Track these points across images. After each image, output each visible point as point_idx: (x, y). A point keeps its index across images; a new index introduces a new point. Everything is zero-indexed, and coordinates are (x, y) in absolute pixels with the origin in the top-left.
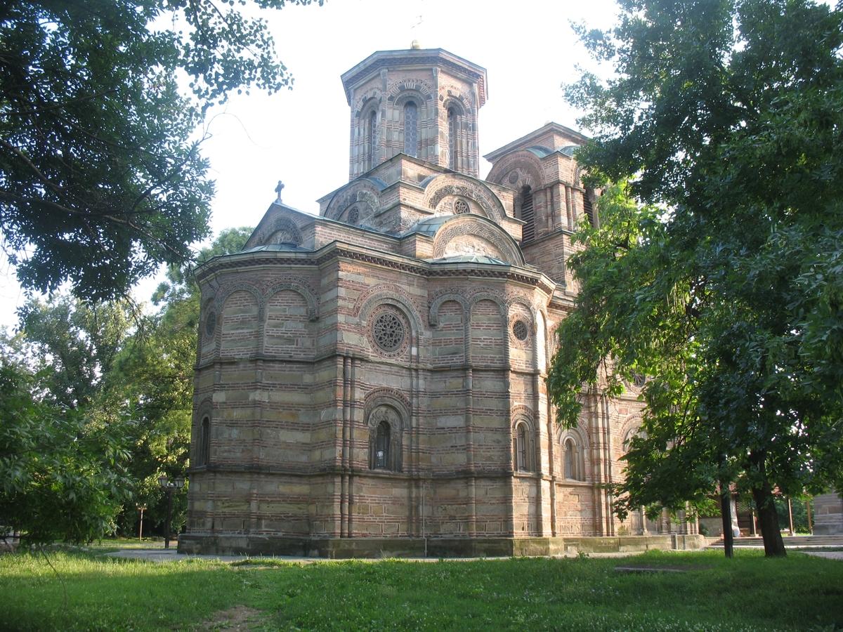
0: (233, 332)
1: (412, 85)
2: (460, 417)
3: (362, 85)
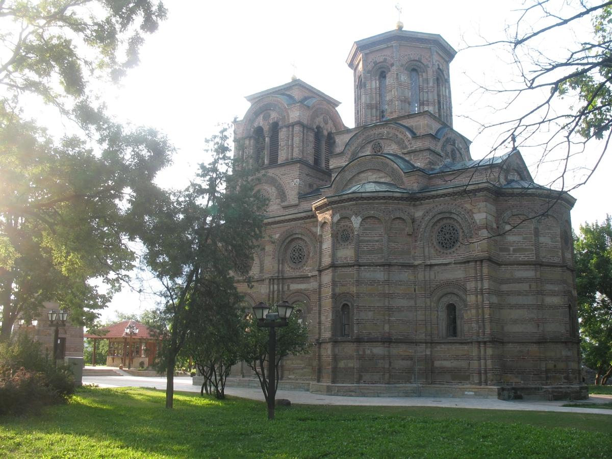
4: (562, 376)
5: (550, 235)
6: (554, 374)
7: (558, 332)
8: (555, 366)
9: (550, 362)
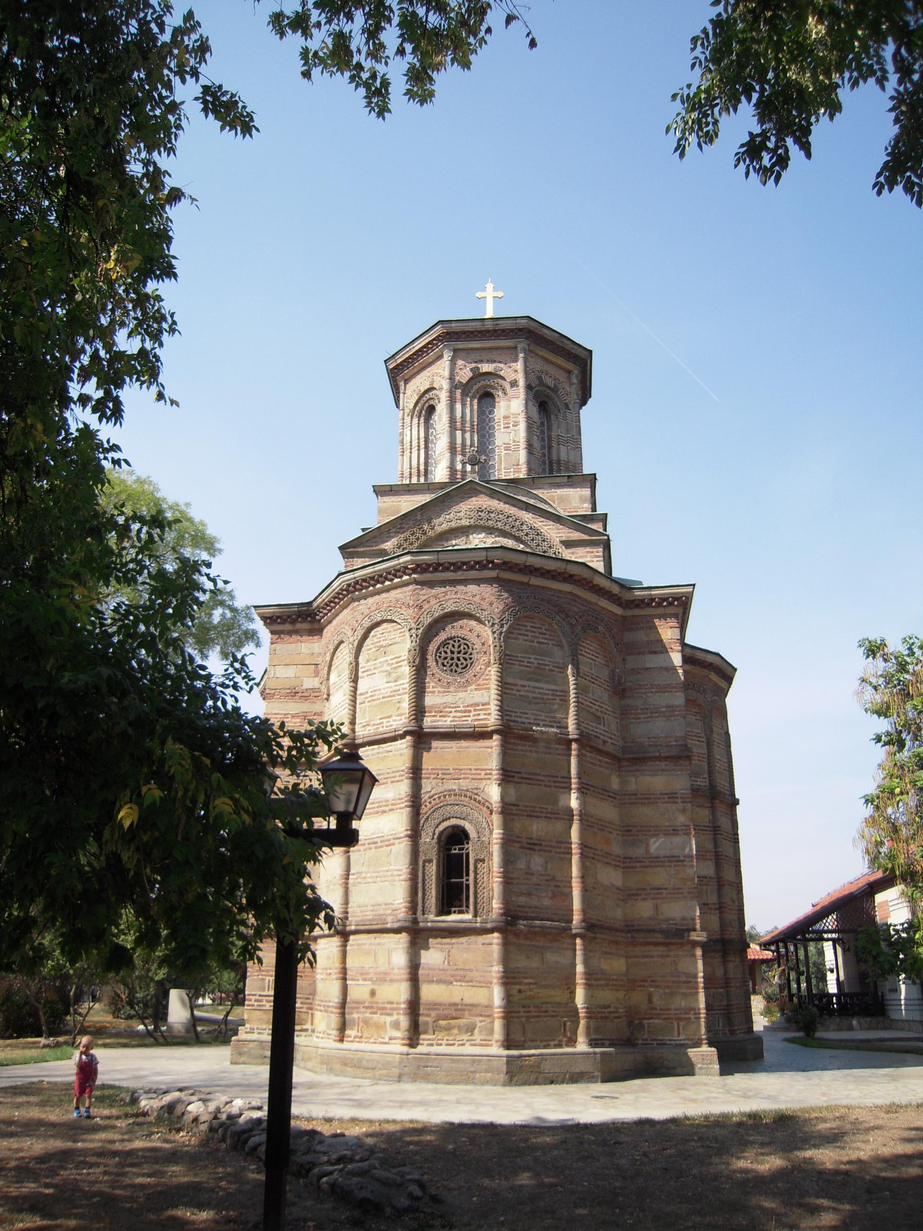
0: (520, 682)
1: (550, 382)
2: (710, 863)
3: (472, 349)
4: (389, 1019)
5: (386, 668)
6: (368, 1015)
7: (386, 904)
8: (373, 993)
9: (361, 982)
